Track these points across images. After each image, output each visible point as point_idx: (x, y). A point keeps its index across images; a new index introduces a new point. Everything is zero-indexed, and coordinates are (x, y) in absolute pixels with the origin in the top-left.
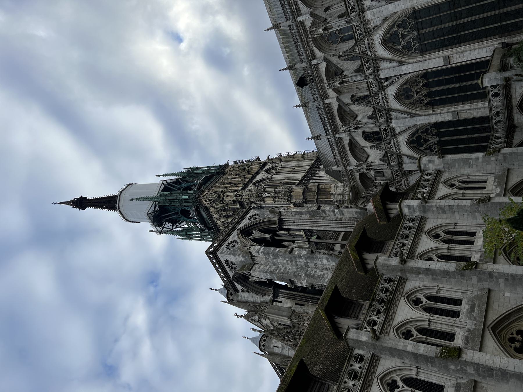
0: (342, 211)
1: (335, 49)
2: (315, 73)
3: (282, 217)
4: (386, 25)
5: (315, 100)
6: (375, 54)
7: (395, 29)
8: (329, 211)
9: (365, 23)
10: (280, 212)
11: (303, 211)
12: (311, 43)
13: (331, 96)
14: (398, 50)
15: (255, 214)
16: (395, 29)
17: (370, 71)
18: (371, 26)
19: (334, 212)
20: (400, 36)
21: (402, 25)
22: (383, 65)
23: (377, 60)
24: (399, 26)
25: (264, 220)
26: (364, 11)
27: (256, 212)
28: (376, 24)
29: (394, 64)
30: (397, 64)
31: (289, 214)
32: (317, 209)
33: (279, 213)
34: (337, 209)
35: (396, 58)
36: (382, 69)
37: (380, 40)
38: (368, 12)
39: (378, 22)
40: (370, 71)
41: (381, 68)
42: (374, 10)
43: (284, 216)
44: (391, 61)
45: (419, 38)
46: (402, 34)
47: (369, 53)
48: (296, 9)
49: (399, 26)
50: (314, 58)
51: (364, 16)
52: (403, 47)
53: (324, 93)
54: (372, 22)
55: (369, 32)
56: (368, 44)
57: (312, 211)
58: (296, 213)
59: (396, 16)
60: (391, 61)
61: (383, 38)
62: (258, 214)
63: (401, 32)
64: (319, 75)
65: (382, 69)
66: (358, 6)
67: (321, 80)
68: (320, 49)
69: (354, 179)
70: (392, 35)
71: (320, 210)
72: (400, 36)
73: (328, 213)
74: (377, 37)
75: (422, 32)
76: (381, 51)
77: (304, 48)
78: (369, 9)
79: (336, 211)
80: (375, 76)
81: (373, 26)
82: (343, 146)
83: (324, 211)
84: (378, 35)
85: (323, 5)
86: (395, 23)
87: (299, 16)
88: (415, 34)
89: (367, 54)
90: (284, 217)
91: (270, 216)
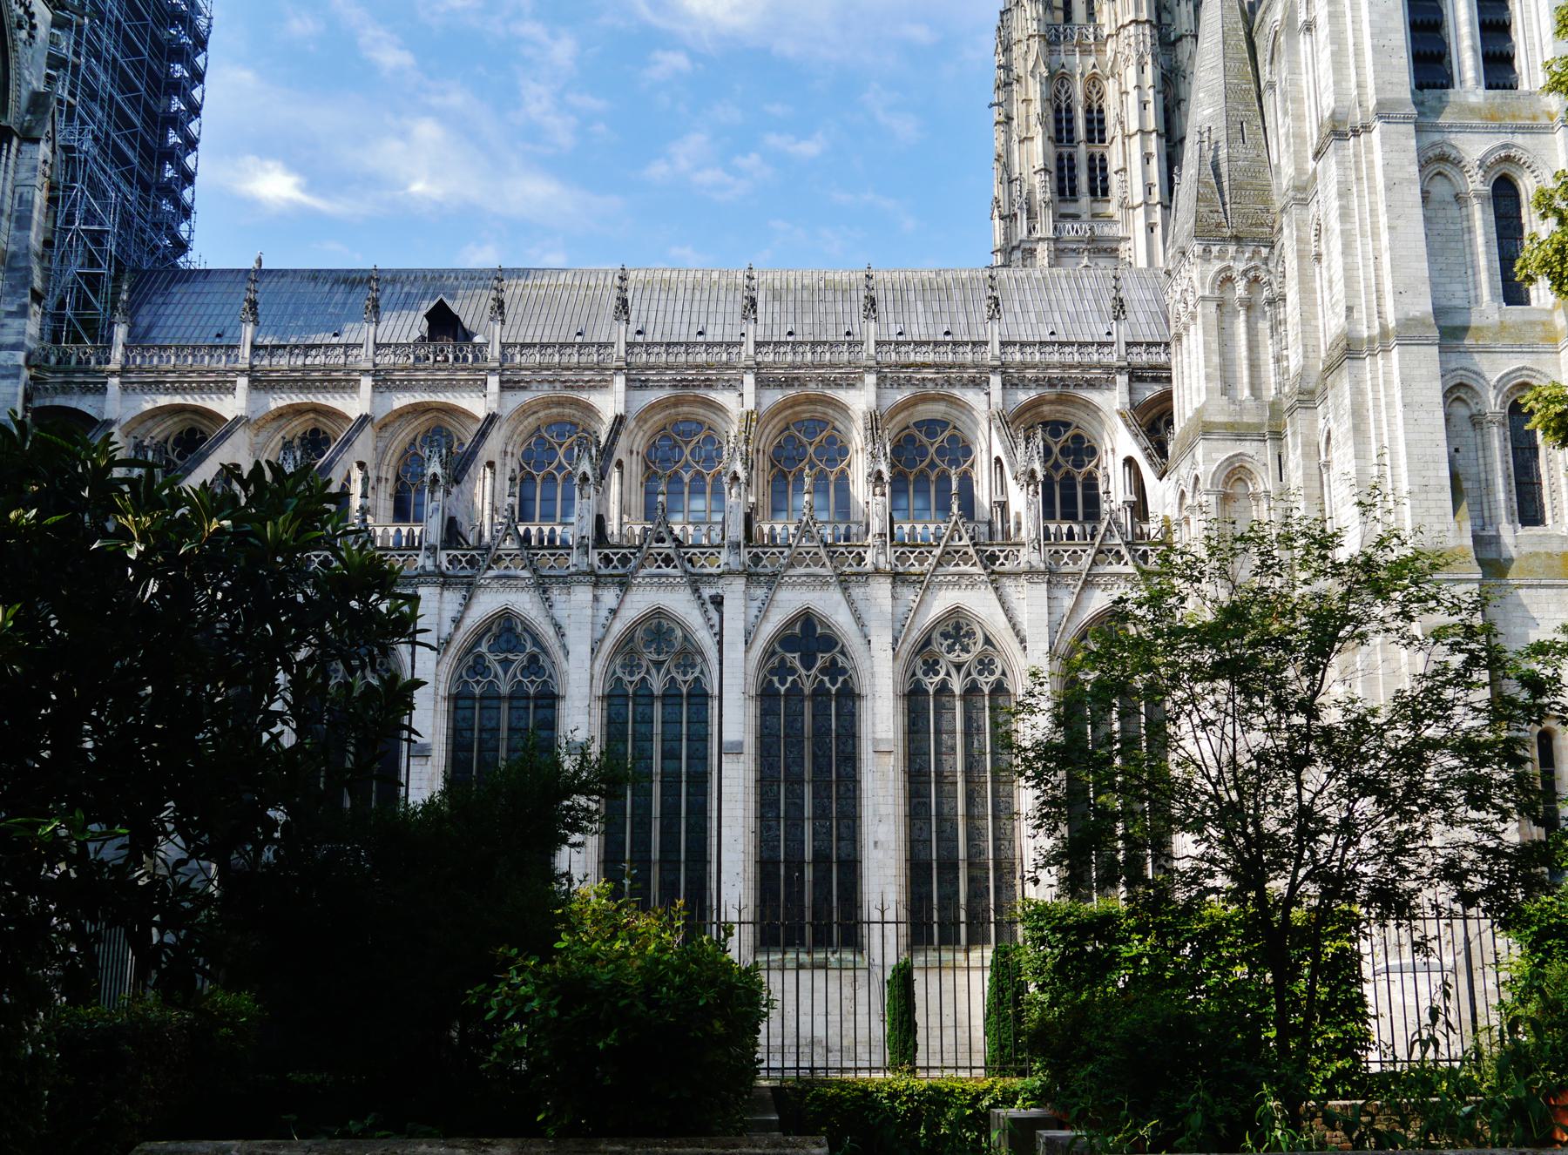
0: (17, 376)
1: (509, 449)
2: (462, 375)
3: (15, 142)
4: (547, 631)
5: (378, 346)
6: (486, 586)
7: (529, 648)
8: (23, 333)
9: (566, 581)
10: (36, 141)
11: (33, 235)
12: (544, 392)
13: (378, 399)
14: (477, 643)
15: (33, 27)
16: (529, 648)
17: (445, 564)
18: (556, 594)
19: (16, 347)
20: (511, 656)
21: (534, 665)
22: (453, 599)
23: (470, 588)
24: (533, 659)
25: (12, 65)
26: (596, 585)
27: (42, 31)
28: (557, 606)
29: (447, 628)
30: (444, 635)
31: (23, 174)
32: (33, 291)
33: (35, 134)
34: (27, 359)
35: (460, 638)
36: (441, 594)
37: (517, 608)
38: (590, 597)
39: (560, 612)
40: (445, 564)
41: (446, 593)
42: (589, 612)
43: (18, 150)
44: (457, 622)
45: (491, 697)
46: (513, 662)
47: (491, 573)
48: (647, 380)
49: (533, 659)
50: (505, 386)
51: (585, 583)
52: (481, 656)
53: (393, 381)
54: (564, 597)
55: (542, 585)
56: (516, 577)
57: (29, 270)
58: (25, 204)
59: (557, 653)
60: (457, 622)
61: (518, 616)
62: (31, 36)
63: (520, 659)
64: (451, 385)
65: (441, 594)
66: (611, 575)
67: (434, 386)
68: (525, 411)
69: (66, 388)
70: (518, 637)
71: (28, 300)
72: (511, 656)
73: (16, 323)
74: (525, 603)
75: (505, 706)
76: (487, 603)
77: (541, 367)
78: (596, 599)
79: (20, 357)
80: (429, 574)
81: (553, 598)
82: (201, 388)
83: (23, 312)
84: (528, 606)
85: (631, 452)
86: (545, 650)
87: (627, 380)
88: (505, 689)
89: (489, 568)
90: (13, 150)
91: (25, 94)
